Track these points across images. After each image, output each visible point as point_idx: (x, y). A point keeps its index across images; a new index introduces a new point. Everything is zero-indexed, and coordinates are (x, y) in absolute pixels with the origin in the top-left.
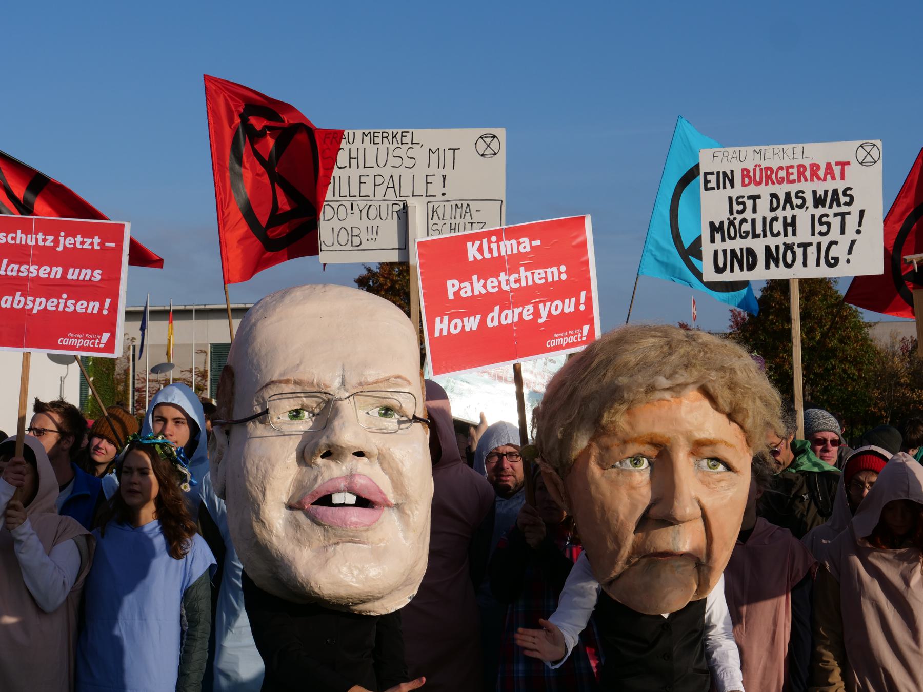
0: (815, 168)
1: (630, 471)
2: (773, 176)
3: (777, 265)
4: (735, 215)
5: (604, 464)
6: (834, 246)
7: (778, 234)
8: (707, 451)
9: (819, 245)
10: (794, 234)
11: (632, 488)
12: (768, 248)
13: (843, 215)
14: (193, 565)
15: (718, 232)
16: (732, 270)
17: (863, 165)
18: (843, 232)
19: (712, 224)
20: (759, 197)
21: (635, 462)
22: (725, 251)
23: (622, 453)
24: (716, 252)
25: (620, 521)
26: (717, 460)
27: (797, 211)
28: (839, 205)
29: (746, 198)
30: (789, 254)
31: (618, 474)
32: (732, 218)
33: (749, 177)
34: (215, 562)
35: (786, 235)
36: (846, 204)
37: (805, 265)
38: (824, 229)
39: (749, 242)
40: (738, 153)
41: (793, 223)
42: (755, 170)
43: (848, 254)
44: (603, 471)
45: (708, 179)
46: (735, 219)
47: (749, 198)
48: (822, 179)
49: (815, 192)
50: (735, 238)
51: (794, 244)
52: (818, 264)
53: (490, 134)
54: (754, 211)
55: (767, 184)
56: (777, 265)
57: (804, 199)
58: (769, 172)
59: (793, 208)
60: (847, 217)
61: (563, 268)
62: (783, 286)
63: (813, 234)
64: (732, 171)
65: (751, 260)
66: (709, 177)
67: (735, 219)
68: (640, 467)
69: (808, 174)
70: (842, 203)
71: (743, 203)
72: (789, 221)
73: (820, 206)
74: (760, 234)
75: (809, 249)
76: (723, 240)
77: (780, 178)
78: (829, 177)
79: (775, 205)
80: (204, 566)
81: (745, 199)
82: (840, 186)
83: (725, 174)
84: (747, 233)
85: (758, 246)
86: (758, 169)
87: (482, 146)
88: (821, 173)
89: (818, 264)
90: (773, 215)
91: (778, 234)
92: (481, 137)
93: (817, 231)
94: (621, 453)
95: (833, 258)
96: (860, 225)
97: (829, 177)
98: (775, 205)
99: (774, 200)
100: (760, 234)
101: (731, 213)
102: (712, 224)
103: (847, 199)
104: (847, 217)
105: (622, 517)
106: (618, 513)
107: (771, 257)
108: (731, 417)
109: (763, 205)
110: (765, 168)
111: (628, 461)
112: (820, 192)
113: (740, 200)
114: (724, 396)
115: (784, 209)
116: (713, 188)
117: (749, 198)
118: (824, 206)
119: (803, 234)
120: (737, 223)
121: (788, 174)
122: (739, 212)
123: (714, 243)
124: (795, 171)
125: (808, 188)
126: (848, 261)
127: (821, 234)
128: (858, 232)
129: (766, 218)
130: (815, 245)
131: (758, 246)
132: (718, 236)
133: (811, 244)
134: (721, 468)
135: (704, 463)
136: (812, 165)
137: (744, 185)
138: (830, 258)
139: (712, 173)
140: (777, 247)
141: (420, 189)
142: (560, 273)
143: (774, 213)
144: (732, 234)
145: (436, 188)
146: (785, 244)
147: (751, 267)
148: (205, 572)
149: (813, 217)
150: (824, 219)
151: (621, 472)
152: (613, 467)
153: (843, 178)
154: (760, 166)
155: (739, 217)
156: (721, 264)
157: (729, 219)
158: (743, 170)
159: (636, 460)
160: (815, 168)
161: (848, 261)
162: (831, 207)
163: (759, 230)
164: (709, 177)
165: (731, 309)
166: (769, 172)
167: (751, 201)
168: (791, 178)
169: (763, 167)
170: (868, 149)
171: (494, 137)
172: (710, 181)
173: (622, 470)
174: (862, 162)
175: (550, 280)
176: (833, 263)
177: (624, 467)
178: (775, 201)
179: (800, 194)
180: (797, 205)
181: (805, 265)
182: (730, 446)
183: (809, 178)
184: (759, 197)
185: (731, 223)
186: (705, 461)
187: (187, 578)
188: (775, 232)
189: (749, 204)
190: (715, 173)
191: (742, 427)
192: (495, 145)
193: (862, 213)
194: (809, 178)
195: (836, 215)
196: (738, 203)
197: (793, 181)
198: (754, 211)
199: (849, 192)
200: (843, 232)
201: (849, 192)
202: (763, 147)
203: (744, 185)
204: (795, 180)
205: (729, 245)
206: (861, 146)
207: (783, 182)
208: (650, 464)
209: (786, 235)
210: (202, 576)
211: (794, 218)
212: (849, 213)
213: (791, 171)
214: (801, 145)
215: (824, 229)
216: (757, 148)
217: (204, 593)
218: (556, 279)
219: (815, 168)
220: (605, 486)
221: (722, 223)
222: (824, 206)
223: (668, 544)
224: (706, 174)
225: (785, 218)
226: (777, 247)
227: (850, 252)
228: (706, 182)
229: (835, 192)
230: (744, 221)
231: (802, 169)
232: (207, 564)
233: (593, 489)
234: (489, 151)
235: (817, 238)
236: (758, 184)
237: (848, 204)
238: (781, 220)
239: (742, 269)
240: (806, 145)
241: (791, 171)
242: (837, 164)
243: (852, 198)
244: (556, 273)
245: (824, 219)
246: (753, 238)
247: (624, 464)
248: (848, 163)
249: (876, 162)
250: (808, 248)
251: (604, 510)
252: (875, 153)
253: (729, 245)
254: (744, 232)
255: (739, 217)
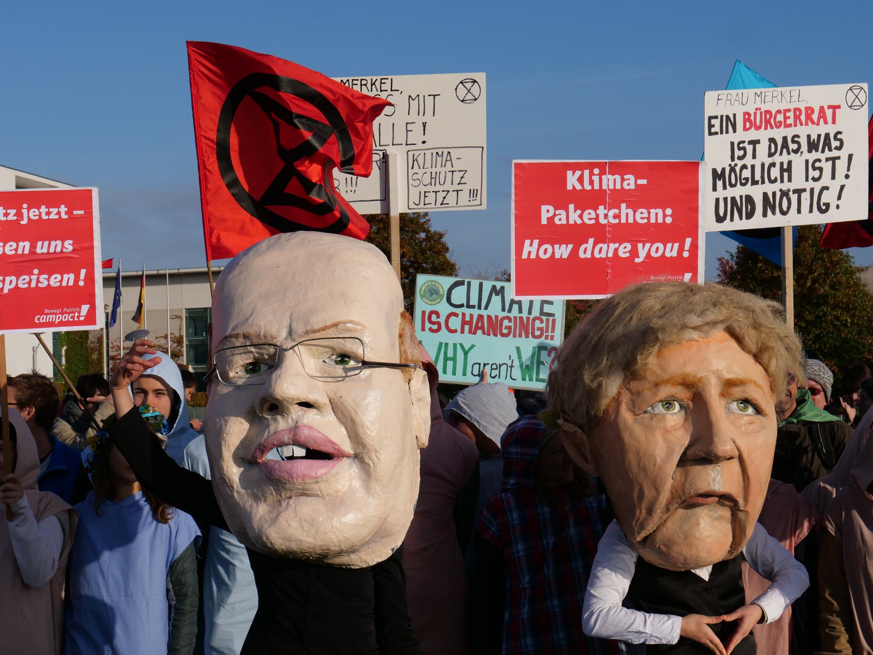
0: (809, 110)
1: (663, 415)
2: (772, 120)
3: (774, 213)
4: (737, 161)
5: (634, 409)
6: (825, 191)
7: (775, 180)
8: (737, 392)
9: (812, 190)
10: (790, 180)
11: (667, 431)
12: (765, 195)
13: (834, 160)
14: (178, 537)
15: (719, 180)
16: (732, 220)
17: (852, 108)
18: (833, 177)
19: (714, 171)
20: (758, 142)
21: (667, 406)
22: (725, 199)
23: (655, 396)
24: (717, 200)
25: (657, 465)
26: (746, 402)
27: (793, 157)
28: (830, 150)
29: (747, 143)
30: (785, 199)
31: (651, 419)
32: (733, 164)
33: (750, 121)
34: (199, 534)
35: (782, 181)
36: (837, 148)
37: (799, 211)
38: (817, 174)
39: (749, 190)
40: (740, 95)
41: (789, 170)
42: (755, 114)
43: (838, 200)
44: (635, 417)
45: (712, 124)
46: (736, 165)
47: (750, 142)
48: (816, 122)
49: (809, 137)
50: (735, 185)
51: (789, 190)
52: (811, 211)
53: (470, 79)
54: (754, 157)
55: (766, 128)
56: (774, 213)
57: (798, 143)
58: (768, 116)
59: (789, 153)
60: (837, 161)
61: (669, 211)
62: (776, 233)
63: (807, 180)
64: (735, 115)
65: (749, 207)
66: (713, 121)
67: (736, 165)
68: (673, 410)
69: (803, 117)
70: (833, 148)
71: (744, 149)
72: (785, 167)
73: (814, 151)
74: (759, 180)
75: (803, 194)
76: (725, 188)
77: (778, 122)
78: (822, 120)
79: (773, 150)
80: (189, 538)
81: (746, 145)
82: (832, 130)
83: (727, 117)
84: (747, 179)
85: (756, 193)
86: (758, 112)
87: (462, 91)
88: (815, 117)
89: (811, 211)
90: (771, 160)
91: (775, 180)
92: (461, 82)
93: (810, 177)
94: (653, 397)
95: (824, 204)
96: (848, 170)
97: (822, 120)
98: (773, 150)
99: (773, 145)
100: (759, 180)
101: (733, 159)
102: (714, 171)
103: (838, 143)
104: (837, 161)
105: (659, 461)
106: (654, 457)
107: (769, 204)
108: (757, 357)
109: (762, 149)
110: (765, 111)
111: (660, 406)
112: (814, 137)
113: (741, 145)
114: (751, 338)
115: (781, 154)
116: (716, 133)
117: (750, 142)
118: (817, 151)
119: (798, 180)
120: (738, 169)
121: (786, 118)
122: (740, 158)
123: (716, 191)
124: (791, 114)
125: (804, 131)
126: (838, 207)
127: (815, 180)
128: (847, 177)
129: (764, 164)
130: (808, 191)
131: (756, 193)
132: (720, 184)
133: (804, 190)
134: (750, 410)
135: (734, 405)
136: (807, 109)
137: (745, 129)
138: (822, 204)
139: (716, 117)
140: (774, 194)
141: (400, 138)
142: (665, 216)
143: (772, 158)
144: (733, 182)
145: (416, 136)
146: (781, 190)
147: (750, 215)
148: (190, 545)
149: (807, 161)
150: (817, 165)
151: (653, 416)
152: (645, 412)
153: (834, 122)
154: (760, 109)
155: (740, 163)
156: (721, 213)
157: (730, 165)
158: (745, 114)
159: (668, 404)
160: (809, 112)
161: (838, 207)
162: (823, 151)
163: (758, 177)
164: (713, 121)
165: (719, 258)
166: (768, 116)
167: (751, 146)
168: (789, 122)
169: (763, 110)
170: (856, 92)
171: (475, 81)
172: (713, 126)
173: (655, 415)
174: (851, 106)
175: (653, 220)
176: (824, 209)
177: (656, 411)
178: (773, 145)
179: (796, 139)
180: (792, 149)
181: (799, 211)
182: (759, 386)
183: (804, 123)
184: (758, 142)
185: (732, 169)
186: (735, 404)
187: (172, 551)
188: (773, 178)
189: (750, 148)
190: (719, 117)
191: (766, 370)
192: (475, 90)
193: (850, 157)
194: (804, 123)
195: (827, 160)
196: (740, 149)
197: (790, 126)
198: (754, 157)
199: (839, 136)
200: (833, 177)
201: (839, 136)
202: (763, 90)
203: (745, 129)
204: (791, 124)
205: (730, 192)
206: (850, 89)
207: (780, 125)
208: (681, 407)
209: (782, 181)
210: (188, 548)
211: (790, 163)
212: (839, 158)
213: (788, 114)
214: (797, 88)
215: (817, 174)
216: (758, 91)
217: (190, 565)
218: (660, 220)
219: (809, 112)
220: (638, 430)
221: (724, 170)
222: (817, 151)
223: (709, 484)
224: (710, 118)
225: (782, 164)
226: (774, 194)
227: (839, 198)
228: (711, 126)
229: (827, 135)
230: (744, 167)
231: (798, 113)
232: (192, 536)
233: (626, 436)
234: (469, 97)
235: (811, 184)
236: (758, 128)
237: (839, 148)
238: (778, 166)
239: (741, 218)
240: (802, 88)
241: (788, 114)
242: (830, 107)
243: (841, 141)
244: (660, 215)
245: (817, 165)
246: (752, 184)
247: (656, 409)
248: (839, 107)
249: (863, 106)
250: (802, 194)
251: (640, 457)
252: (863, 97)
253: (730, 192)
254: (744, 179)
255: (740, 163)
